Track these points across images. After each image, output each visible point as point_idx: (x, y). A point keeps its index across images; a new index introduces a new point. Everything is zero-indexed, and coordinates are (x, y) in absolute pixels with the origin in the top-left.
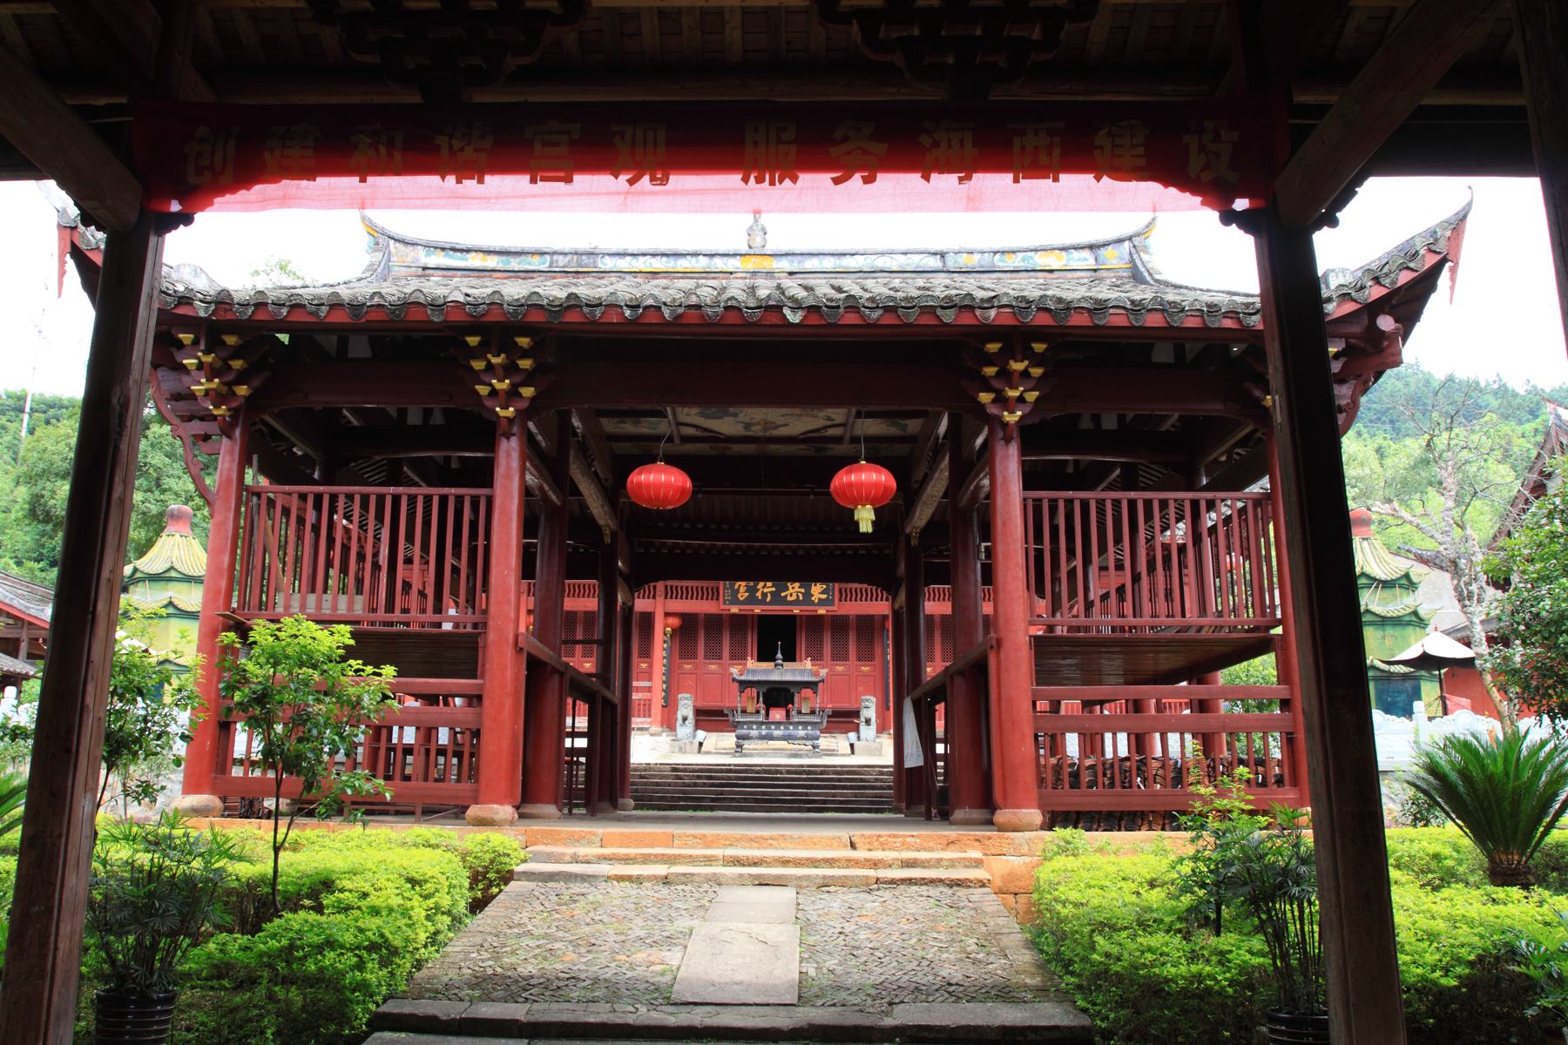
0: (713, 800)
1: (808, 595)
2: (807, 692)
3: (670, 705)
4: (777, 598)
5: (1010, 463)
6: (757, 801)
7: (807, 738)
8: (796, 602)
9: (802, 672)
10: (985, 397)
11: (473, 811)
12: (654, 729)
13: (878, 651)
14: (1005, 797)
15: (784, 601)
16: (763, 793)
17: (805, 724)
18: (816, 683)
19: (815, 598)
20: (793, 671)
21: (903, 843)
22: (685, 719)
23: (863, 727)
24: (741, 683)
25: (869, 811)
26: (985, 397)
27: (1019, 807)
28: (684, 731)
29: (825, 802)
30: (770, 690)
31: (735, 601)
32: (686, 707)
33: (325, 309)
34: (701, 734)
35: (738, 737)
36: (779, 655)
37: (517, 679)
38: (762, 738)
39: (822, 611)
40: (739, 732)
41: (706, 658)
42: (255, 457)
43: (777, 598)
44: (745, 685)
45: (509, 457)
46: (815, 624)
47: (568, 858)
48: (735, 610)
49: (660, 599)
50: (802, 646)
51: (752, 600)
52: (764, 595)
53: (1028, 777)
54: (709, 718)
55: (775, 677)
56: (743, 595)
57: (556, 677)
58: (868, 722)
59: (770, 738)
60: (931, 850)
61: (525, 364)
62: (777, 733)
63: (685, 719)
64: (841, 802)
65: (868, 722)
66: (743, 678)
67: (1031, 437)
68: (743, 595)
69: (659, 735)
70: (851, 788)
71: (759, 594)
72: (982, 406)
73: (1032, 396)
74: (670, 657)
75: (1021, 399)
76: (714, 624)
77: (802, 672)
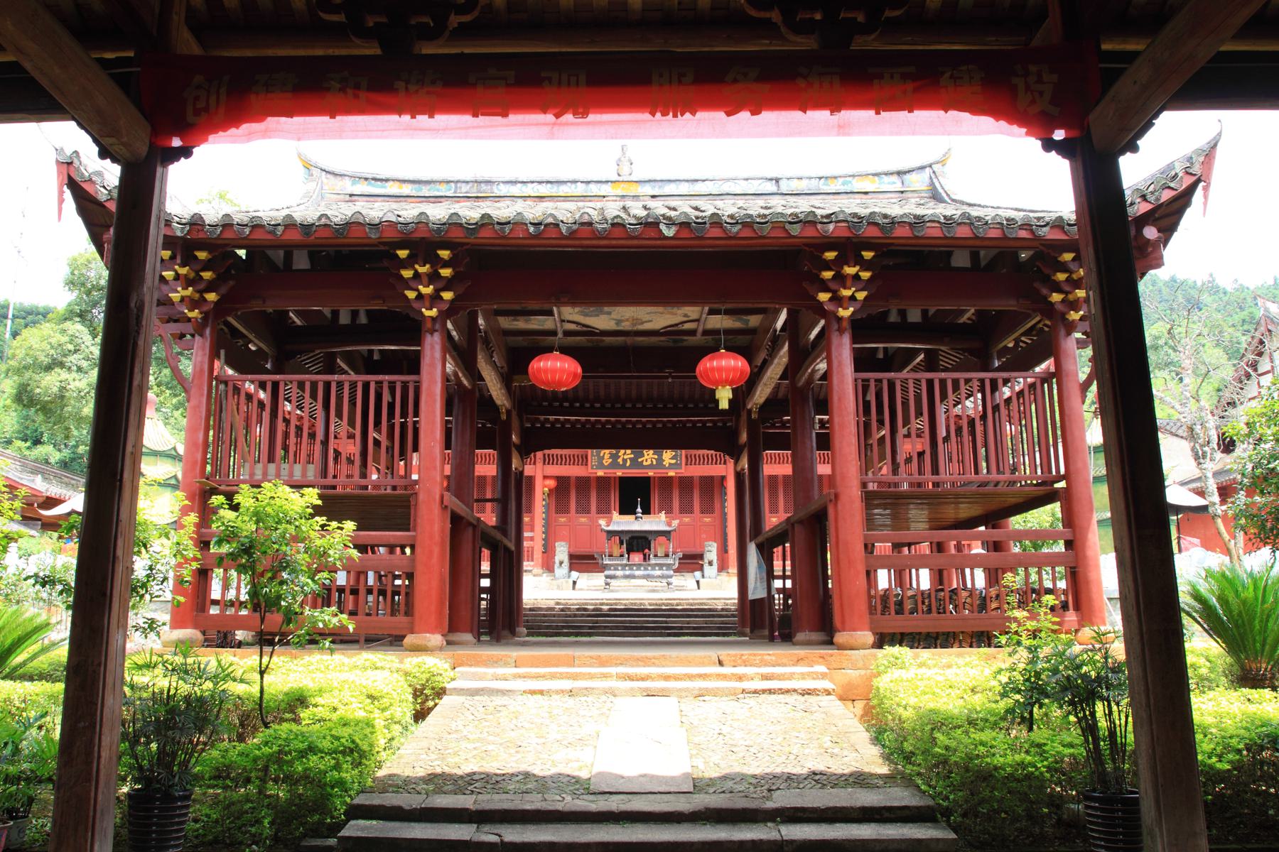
0: (590, 628)
1: (660, 460)
3: (548, 551)
4: (635, 463)
5: (844, 349)
6: (626, 628)
7: (662, 577)
8: (651, 467)
10: (824, 297)
11: (409, 639)
13: (717, 505)
14: (843, 622)
15: (641, 465)
16: (631, 622)
17: (661, 566)
18: (669, 532)
19: (666, 463)
21: (762, 661)
22: (561, 563)
23: (706, 567)
24: (609, 532)
25: (717, 635)
26: (824, 297)
27: (854, 630)
28: (561, 571)
29: (681, 628)
30: (632, 538)
32: (561, 553)
33: (280, 228)
34: (575, 574)
35: (607, 577)
36: (639, 510)
37: (442, 531)
39: (671, 474)
40: (607, 573)
41: (577, 512)
42: (222, 352)
43: (635, 463)
45: (432, 351)
46: (666, 482)
47: (489, 677)
48: (600, 473)
49: (539, 464)
50: (655, 501)
53: (862, 606)
54: (583, 561)
56: (607, 461)
57: (470, 530)
58: (710, 563)
59: (633, 577)
60: (784, 665)
61: (446, 272)
62: (637, 573)
63: (561, 563)
64: (694, 628)
65: (710, 563)
66: (610, 528)
67: (861, 328)
70: (702, 616)
71: (620, 461)
72: (821, 304)
73: (861, 296)
74: (547, 512)
75: (853, 298)
76: (583, 484)
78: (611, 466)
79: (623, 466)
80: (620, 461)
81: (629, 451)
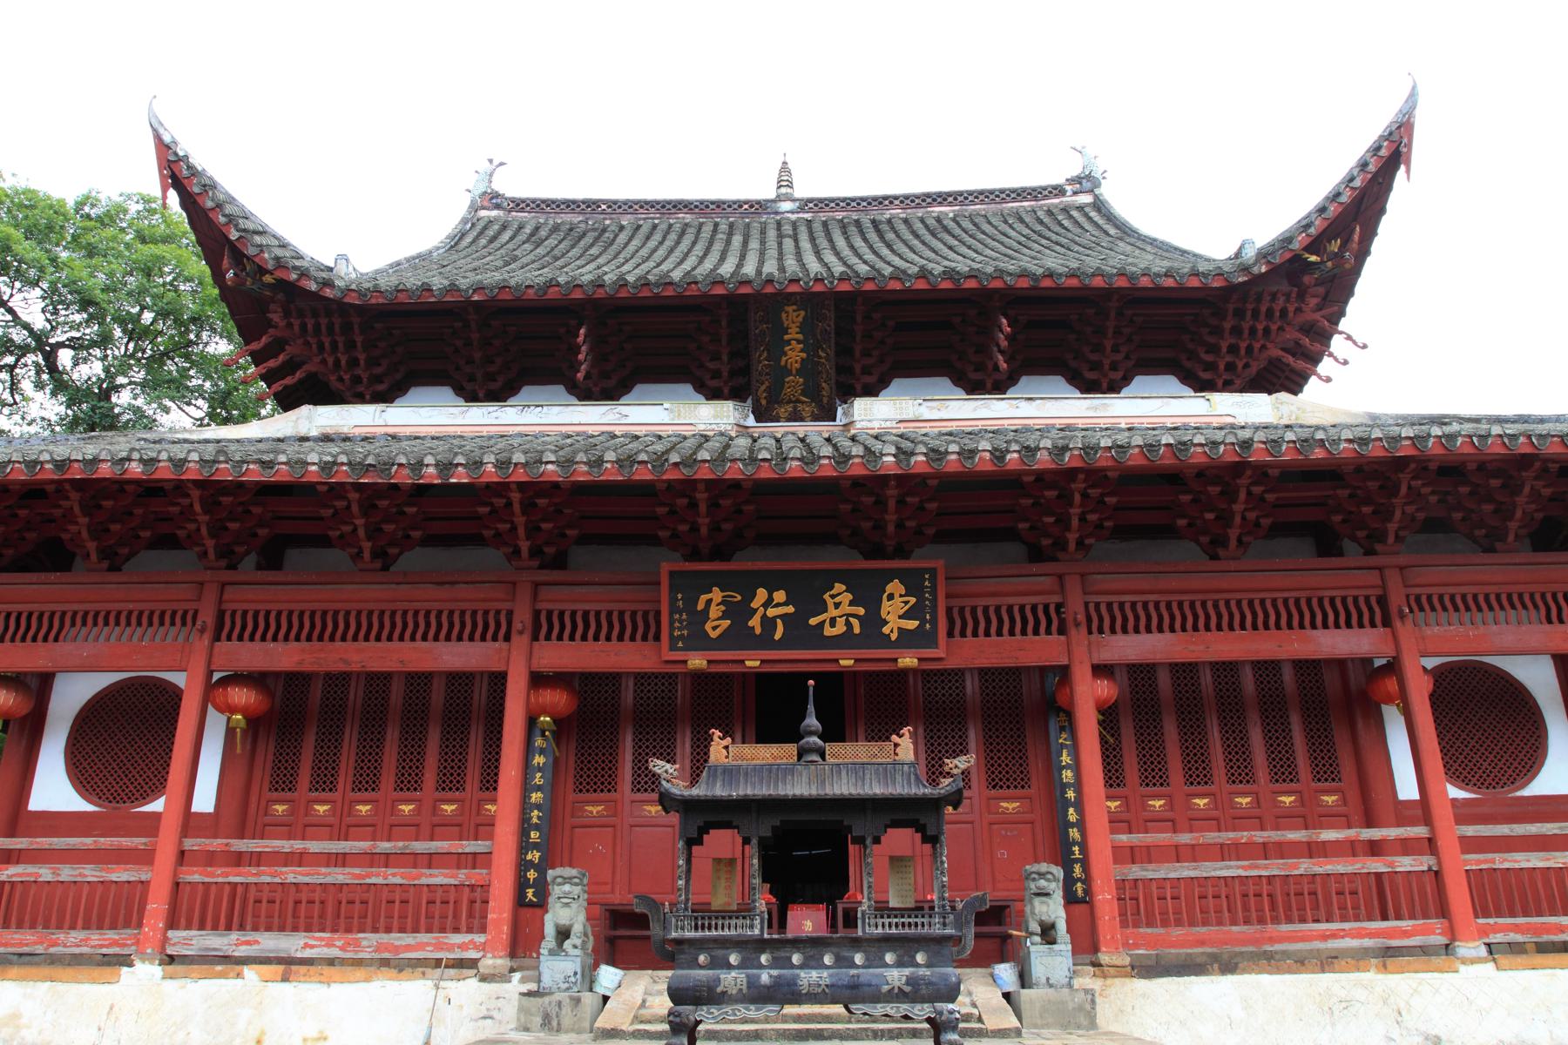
1: (873, 621)
2: (900, 839)
3: (530, 902)
4: (800, 632)
7: (913, 993)
9: (889, 770)
12: (490, 963)
13: (1035, 766)
15: (816, 638)
17: (905, 946)
18: (933, 805)
19: (892, 628)
20: (858, 769)
24: (689, 807)
28: (558, 968)
31: (697, 640)
32: (567, 907)
34: (608, 976)
36: (812, 721)
38: (760, 996)
39: (908, 661)
43: (800, 632)
44: (702, 817)
48: (697, 662)
49: (520, 642)
51: (738, 636)
52: (768, 623)
55: (800, 787)
56: (716, 625)
58: (1047, 933)
59: (783, 993)
62: (810, 978)
63: (563, 934)
66: (697, 791)
68: (716, 625)
69: (503, 978)
71: (755, 622)
74: (553, 789)
77: (889, 770)
78: (725, 641)
79: (765, 641)
80: (755, 622)
81: (780, 596)
